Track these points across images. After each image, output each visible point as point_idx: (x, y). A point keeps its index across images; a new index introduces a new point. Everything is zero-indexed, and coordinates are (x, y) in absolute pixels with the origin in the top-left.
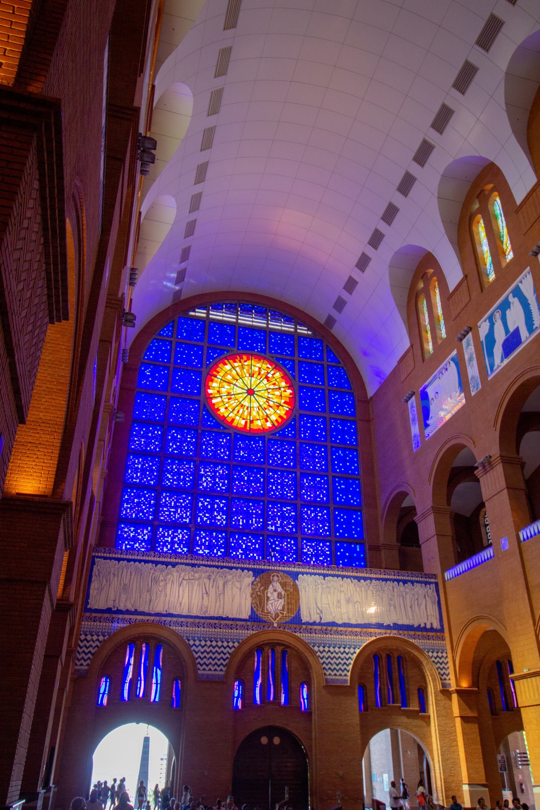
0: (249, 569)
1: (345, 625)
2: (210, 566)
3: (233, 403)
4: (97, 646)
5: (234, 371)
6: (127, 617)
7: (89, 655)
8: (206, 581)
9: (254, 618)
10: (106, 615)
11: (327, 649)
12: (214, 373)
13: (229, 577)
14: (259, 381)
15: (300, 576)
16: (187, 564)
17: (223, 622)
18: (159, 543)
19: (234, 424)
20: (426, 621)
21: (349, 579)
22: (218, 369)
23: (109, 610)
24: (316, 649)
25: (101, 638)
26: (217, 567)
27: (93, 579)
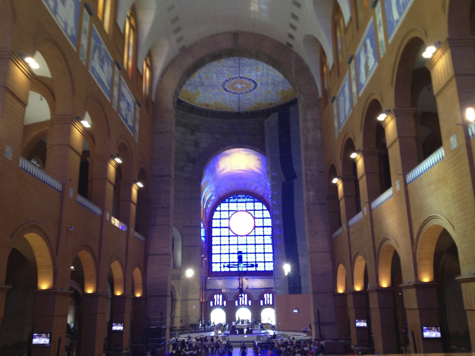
0: (237, 279)
8: (228, 282)
15: (248, 279)
23: (210, 289)
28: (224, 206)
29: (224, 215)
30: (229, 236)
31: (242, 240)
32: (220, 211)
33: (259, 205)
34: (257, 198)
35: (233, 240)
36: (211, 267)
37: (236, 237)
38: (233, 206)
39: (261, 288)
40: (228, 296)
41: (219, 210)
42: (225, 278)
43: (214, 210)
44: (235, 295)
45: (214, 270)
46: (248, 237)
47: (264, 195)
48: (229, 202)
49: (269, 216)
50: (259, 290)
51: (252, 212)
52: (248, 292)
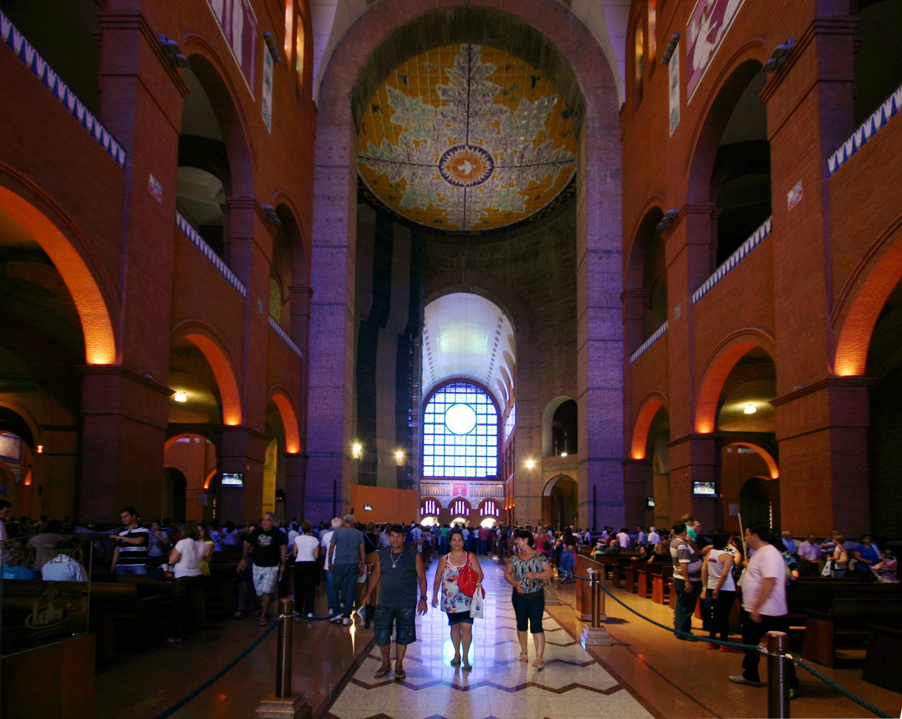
28: (440, 397)
29: (440, 408)
31: (460, 440)
32: (435, 403)
33: (482, 398)
34: (482, 387)
35: (450, 440)
36: (423, 471)
38: (450, 398)
41: (433, 401)
43: (426, 402)
46: (467, 436)
48: (445, 393)
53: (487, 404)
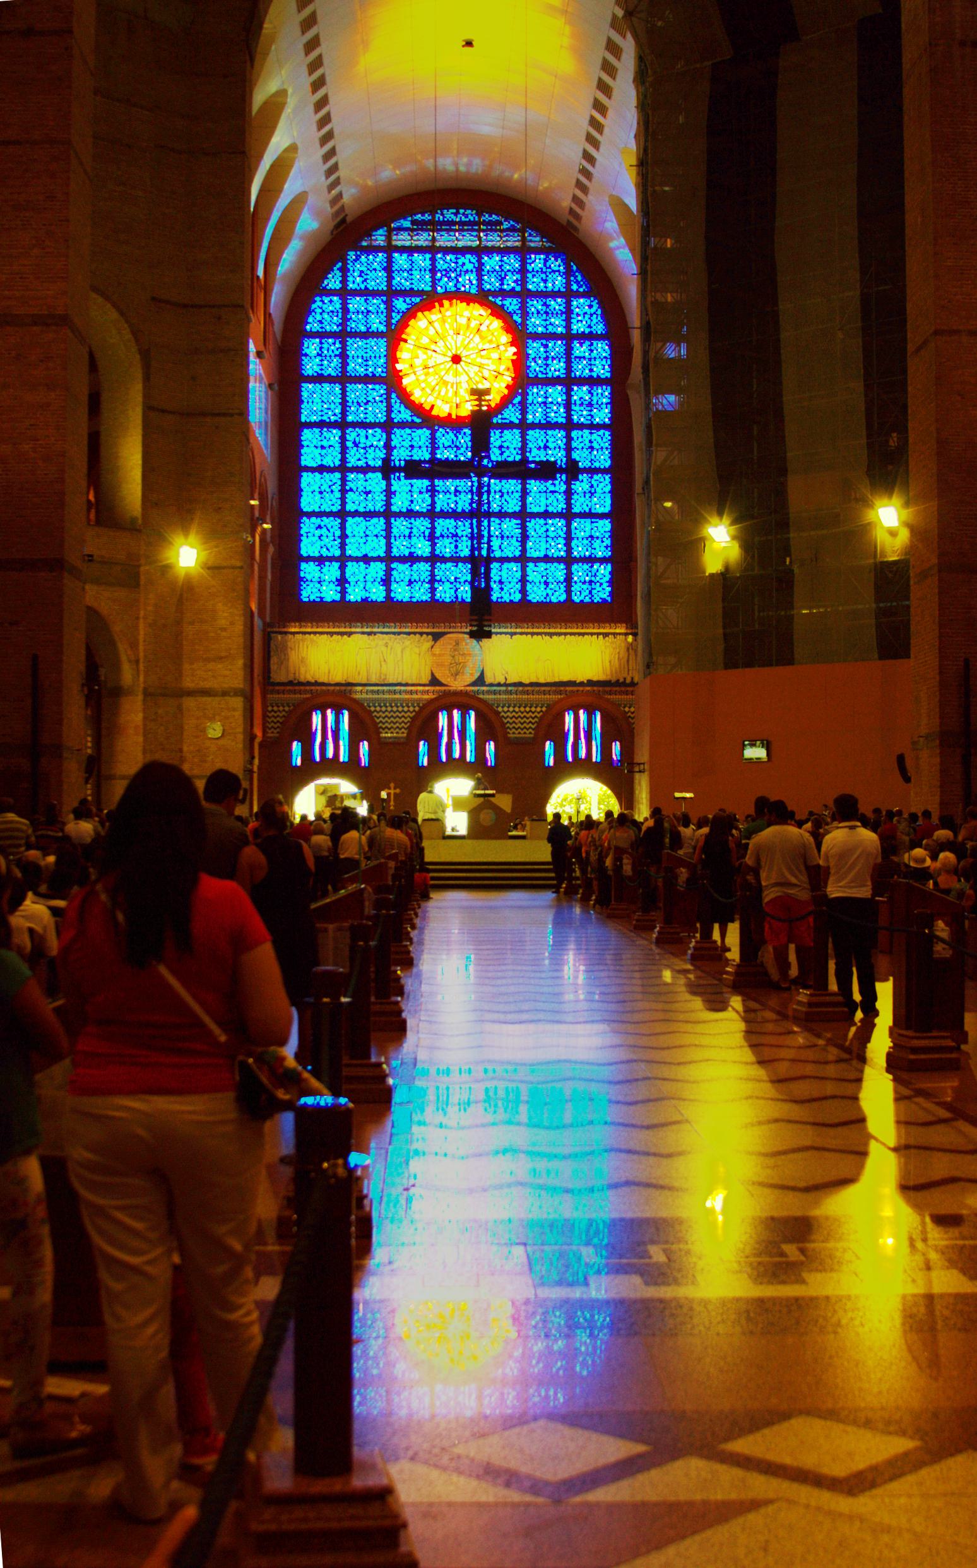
0: (428, 634)
1: (532, 684)
2: (387, 633)
3: (432, 380)
4: (284, 716)
5: (431, 328)
6: (308, 688)
7: (278, 724)
8: (384, 649)
9: (434, 681)
10: (288, 688)
11: (511, 709)
12: (404, 336)
13: (407, 643)
14: (467, 340)
16: (363, 633)
17: (403, 688)
18: (349, 583)
19: (434, 413)
20: (625, 675)
21: (540, 637)
22: (408, 330)
23: (291, 683)
24: (500, 709)
25: (287, 709)
26: (394, 633)
27: (272, 654)
30: (388, 426)
32: (344, 293)
37: (425, 433)
39: (549, 680)
40: (380, 718)
42: (365, 630)
44: (418, 714)
45: (309, 593)
47: (578, 210)
49: (600, 328)
50: (539, 693)
51: (512, 304)
52: (480, 700)
53: (568, 295)
